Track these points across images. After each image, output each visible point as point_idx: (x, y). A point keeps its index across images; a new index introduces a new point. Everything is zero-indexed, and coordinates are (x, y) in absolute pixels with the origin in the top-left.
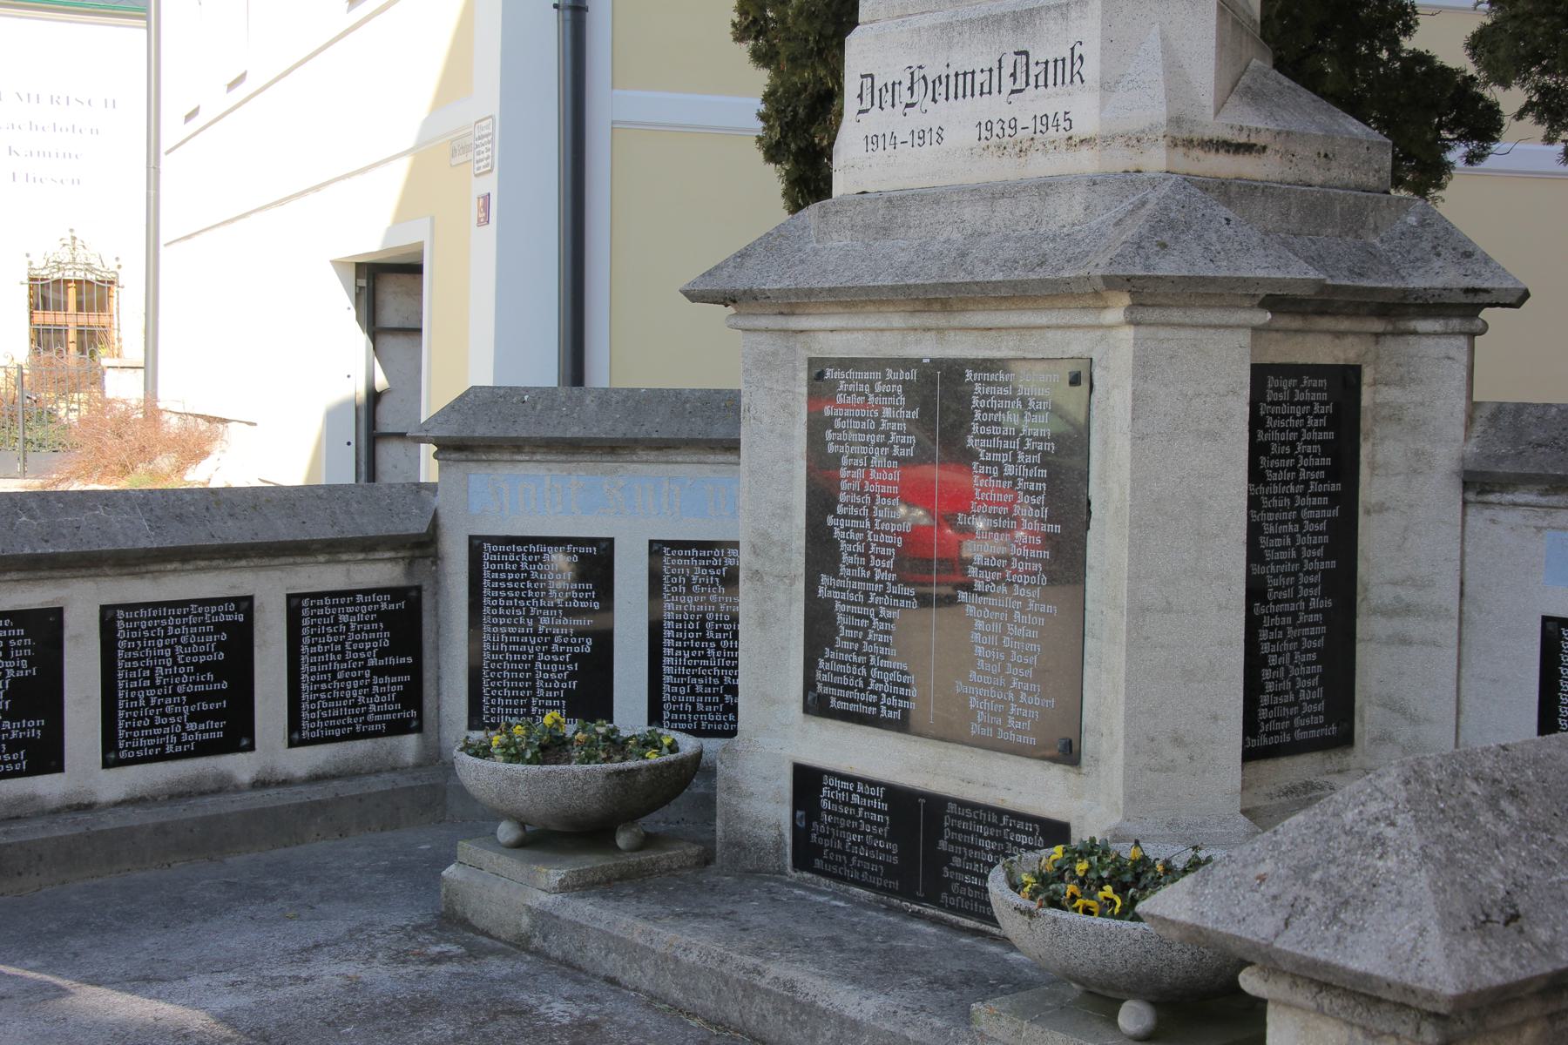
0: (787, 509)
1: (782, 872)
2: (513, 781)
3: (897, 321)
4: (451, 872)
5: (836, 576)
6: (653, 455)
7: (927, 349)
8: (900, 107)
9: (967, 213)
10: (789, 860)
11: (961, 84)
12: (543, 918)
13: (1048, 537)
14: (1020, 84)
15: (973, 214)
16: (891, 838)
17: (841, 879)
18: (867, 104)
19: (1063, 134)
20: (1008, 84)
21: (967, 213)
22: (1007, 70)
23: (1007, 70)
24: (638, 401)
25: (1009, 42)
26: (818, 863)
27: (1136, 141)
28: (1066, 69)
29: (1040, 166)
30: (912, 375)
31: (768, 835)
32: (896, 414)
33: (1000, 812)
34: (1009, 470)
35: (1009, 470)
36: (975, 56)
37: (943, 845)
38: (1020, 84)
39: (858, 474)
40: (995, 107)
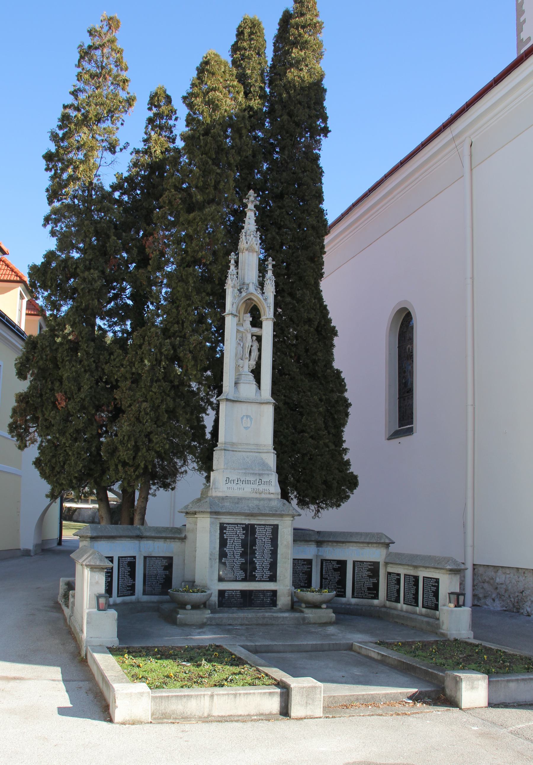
0: (215, 548)
1: (215, 608)
2: (204, 596)
3: (243, 518)
4: (179, 616)
5: (226, 558)
6: (119, 539)
7: (247, 522)
8: (235, 484)
9: (255, 502)
10: (217, 606)
11: (249, 482)
12: (210, 619)
13: (271, 550)
14: (260, 483)
15: (257, 502)
16: (241, 598)
17: (231, 607)
18: (228, 482)
19: (268, 492)
20: (258, 483)
21: (255, 502)
22: (257, 482)
23: (257, 482)
24: (157, 529)
25: (258, 478)
26: (224, 605)
27: (278, 494)
28: (269, 483)
29: (263, 496)
30: (244, 526)
31: (213, 603)
32: (240, 532)
33: (264, 591)
34: (263, 540)
35: (263, 540)
36: (252, 479)
37: (252, 597)
38: (260, 483)
39: (232, 541)
40: (255, 486)
